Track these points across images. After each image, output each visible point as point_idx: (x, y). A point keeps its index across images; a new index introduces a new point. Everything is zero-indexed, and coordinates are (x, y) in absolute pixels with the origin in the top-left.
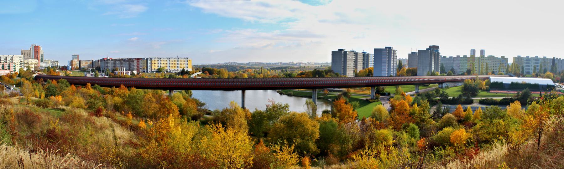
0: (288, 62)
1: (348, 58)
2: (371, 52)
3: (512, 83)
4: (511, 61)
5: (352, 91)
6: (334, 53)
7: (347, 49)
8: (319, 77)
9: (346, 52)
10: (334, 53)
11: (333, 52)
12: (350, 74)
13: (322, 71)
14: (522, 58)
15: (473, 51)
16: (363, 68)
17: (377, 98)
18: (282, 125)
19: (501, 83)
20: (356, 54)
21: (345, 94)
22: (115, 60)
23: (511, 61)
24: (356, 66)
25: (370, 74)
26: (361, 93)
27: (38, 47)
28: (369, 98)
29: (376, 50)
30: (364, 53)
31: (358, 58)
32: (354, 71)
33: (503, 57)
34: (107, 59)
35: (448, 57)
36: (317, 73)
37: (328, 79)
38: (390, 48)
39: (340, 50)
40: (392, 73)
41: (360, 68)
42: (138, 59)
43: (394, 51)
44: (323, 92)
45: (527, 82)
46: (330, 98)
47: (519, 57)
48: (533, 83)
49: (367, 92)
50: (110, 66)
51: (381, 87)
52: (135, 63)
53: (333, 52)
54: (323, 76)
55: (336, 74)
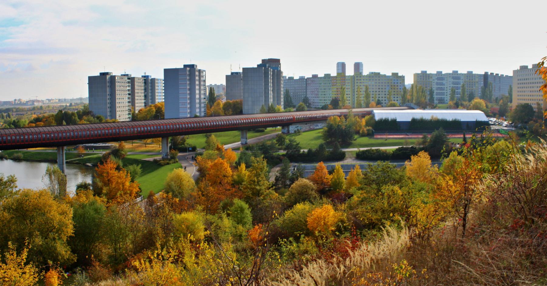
0: (11, 99)
1: (117, 88)
2: (159, 76)
3: (414, 121)
4: (409, 81)
5: (127, 146)
6: (92, 80)
7: (116, 72)
8: (68, 124)
9: (113, 78)
10: (92, 80)
11: (90, 78)
12: (123, 115)
13: (73, 114)
14: (430, 76)
15: (342, 66)
16: (146, 104)
17: (173, 158)
18: (6, 214)
19: (394, 121)
20: (132, 80)
21: (116, 153)
23: (409, 81)
24: (132, 102)
25: (159, 114)
26: (143, 149)
28: (158, 158)
29: (167, 72)
30: (146, 79)
31: (136, 87)
32: (130, 110)
33: (395, 75)
35: (296, 77)
36: (64, 117)
37: (83, 127)
38: (192, 67)
39: (103, 75)
40: (198, 110)
41: (140, 104)
43: (200, 71)
44: (76, 152)
45: (440, 117)
46: (89, 160)
47: (424, 73)
48: (450, 118)
49: (154, 148)
51: (180, 138)
53: (90, 78)
54: (75, 123)
55: (98, 118)
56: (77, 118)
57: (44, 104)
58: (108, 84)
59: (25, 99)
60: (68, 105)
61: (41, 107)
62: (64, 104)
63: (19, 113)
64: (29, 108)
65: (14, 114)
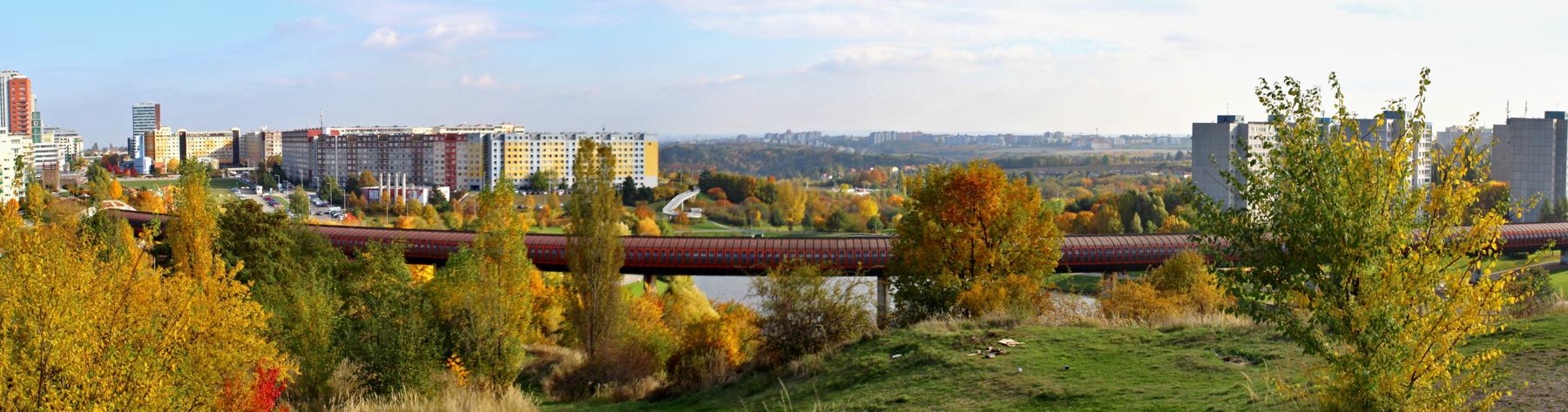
22: (354, 138)
27: (24, 82)
34: (322, 137)
39: (1225, 120)
42: (451, 138)
50: (335, 164)
52: (439, 149)
56: (1163, 209)
57: (1113, 147)
58: (1232, 142)
59: (1070, 129)
60: (1174, 153)
61: (1105, 159)
62: (1165, 152)
63: (1051, 170)
64: (1075, 158)
65: (1041, 171)
